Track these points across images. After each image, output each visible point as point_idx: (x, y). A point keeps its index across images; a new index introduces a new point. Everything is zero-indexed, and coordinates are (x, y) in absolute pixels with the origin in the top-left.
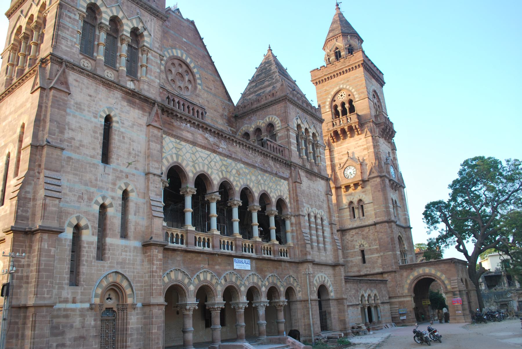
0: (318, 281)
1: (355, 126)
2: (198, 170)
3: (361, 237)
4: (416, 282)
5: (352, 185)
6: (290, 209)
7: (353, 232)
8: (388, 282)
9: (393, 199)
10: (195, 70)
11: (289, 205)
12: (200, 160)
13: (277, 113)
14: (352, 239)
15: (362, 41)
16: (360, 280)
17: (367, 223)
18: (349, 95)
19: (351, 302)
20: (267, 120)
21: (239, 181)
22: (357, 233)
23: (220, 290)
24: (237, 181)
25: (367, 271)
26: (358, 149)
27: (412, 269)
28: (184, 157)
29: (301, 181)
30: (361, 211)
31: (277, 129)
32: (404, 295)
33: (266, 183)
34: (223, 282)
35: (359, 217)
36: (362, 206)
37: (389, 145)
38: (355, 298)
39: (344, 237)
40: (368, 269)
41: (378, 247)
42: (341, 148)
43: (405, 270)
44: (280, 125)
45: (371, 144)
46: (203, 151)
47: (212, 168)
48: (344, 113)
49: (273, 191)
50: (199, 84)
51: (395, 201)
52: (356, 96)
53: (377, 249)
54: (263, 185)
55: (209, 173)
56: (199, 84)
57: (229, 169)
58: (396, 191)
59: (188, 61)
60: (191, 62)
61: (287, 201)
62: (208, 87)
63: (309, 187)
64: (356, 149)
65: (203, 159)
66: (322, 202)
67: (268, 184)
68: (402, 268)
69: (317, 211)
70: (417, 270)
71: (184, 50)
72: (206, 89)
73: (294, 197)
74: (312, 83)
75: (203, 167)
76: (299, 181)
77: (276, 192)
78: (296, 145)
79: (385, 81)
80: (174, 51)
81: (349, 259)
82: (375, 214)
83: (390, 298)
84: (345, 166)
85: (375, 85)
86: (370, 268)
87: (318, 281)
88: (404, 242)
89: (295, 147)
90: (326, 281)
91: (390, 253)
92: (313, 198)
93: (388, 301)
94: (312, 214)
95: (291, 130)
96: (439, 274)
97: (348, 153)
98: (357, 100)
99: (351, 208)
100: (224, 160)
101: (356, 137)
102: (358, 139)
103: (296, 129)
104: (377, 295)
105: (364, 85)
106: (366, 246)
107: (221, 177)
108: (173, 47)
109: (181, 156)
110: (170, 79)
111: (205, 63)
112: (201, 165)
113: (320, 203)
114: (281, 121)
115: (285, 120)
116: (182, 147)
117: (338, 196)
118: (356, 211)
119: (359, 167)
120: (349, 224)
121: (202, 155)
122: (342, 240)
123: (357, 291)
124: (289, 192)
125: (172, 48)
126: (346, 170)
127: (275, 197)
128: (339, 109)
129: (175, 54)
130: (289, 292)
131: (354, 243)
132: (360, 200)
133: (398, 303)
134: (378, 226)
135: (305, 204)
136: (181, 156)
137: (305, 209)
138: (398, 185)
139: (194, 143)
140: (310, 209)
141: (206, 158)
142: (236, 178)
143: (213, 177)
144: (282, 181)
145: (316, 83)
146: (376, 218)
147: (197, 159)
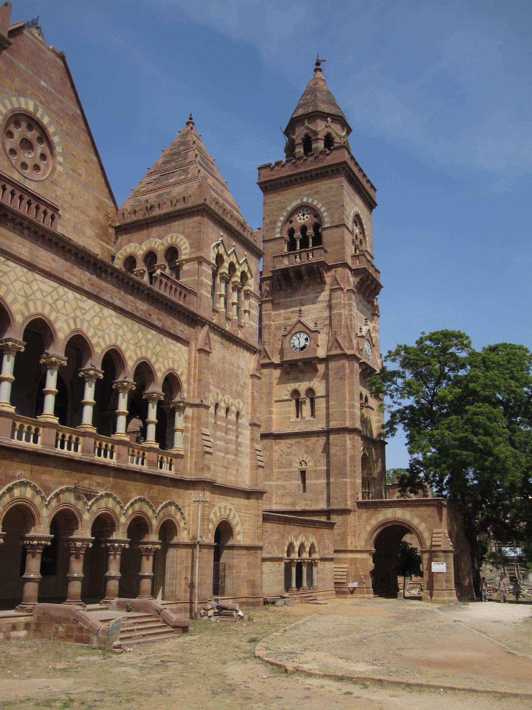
0: (218, 515)
2: (33, 311)
3: (304, 449)
4: (379, 530)
6: (187, 392)
8: (335, 527)
10: (56, 139)
11: (185, 386)
12: (39, 294)
13: (186, 231)
14: (289, 450)
15: (349, 131)
16: (290, 519)
17: (315, 429)
19: (270, 553)
20: (168, 240)
21: (103, 337)
22: (299, 443)
23: (45, 515)
24: (99, 338)
25: (306, 504)
28: (11, 287)
29: (211, 349)
31: (183, 257)
33: (150, 345)
34: (54, 503)
37: (369, 307)
38: (278, 547)
42: (291, 301)
43: (364, 510)
44: (188, 251)
46: (46, 280)
47: (58, 311)
48: (304, 243)
49: (161, 359)
50: (60, 164)
52: (326, 220)
54: (143, 349)
55: (52, 318)
56: (60, 164)
57: (88, 317)
59: (46, 121)
60: (50, 123)
61: (183, 378)
62: (74, 171)
63: (224, 359)
65: (45, 294)
66: (241, 386)
67: (154, 347)
68: (361, 505)
69: (231, 400)
71: (41, 102)
72: (71, 173)
73: (195, 374)
74: (258, 186)
75: (43, 307)
76: (207, 348)
77: (166, 362)
78: (210, 289)
79: (377, 201)
80: (22, 100)
84: (293, 332)
86: (311, 501)
87: (218, 515)
89: (208, 292)
90: (231, 516)
92: (227, 379)
94: (222, 404)
95: (204, 263)
98: (327, 225)
100: (81, 301)
103: (214, 262)
104: (316, 545)
106: (310, 466)
107: (73, 327)
108: (21, 93)
109: (5, 285)
110: (8, 148)
111: (75, 129)
112: (39, 304)
113: (239, 388)
114: (191, 245)
115: (197, 244)
116: (9, 269)
121: (43, 286)
123: (283, 536)
124: (189, 364)
125: (19, 95)
127: (163, 370)
128: (298, 234)
129: (24, 106)
130: (168, 529)
131: (292, 457)
135: (211, 387)
136: (5, 285)
137: (211, 395)
139: (31, 267)
140: (220, 396)
141: (50, 293)
142: (98, 331)
143: (57, 326)
144: (179, 345)
147: (33, 293)
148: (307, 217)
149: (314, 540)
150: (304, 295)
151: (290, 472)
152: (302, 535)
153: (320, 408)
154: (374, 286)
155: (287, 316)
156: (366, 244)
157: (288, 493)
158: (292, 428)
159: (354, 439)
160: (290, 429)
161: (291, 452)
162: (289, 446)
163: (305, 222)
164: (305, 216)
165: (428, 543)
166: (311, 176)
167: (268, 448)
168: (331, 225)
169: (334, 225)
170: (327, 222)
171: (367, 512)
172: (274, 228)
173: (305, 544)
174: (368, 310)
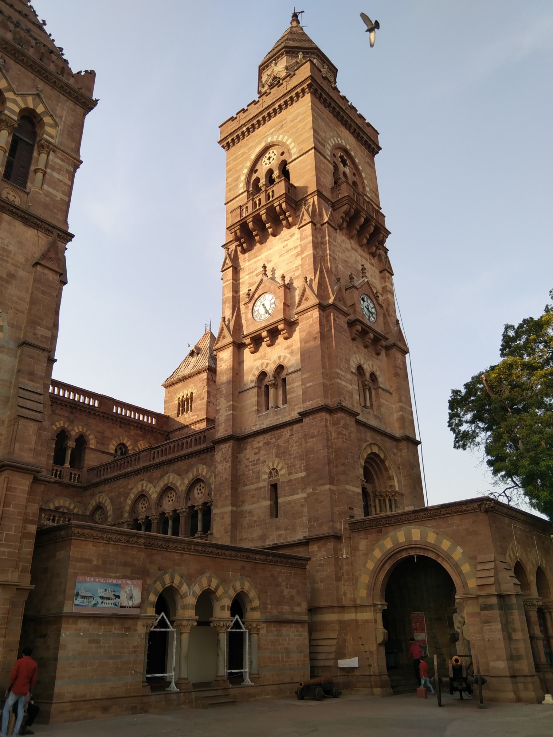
1: (280, 205)
3: (274, 451)
4: (387, 567)
5: (264, 334)
7: (259, 442)
9: (365, 367)
14: (257, 457)
17: (288, 419)
18: (283, 154)
22: (268, 443)
25: (280, 536)
26: (288, 256)
27: (380, 532)
30: (280, 392)
32: (358, 602)
35: (277, 407)
36: (284, 380)
37: (375, 261)
39: (242, 455)
40: (282, 532)
41: (303, 474)
42: (256, 262)
45: (310, 238)
51: (373, 375)
52: (293, 152)
53: (303, 478)
58: (378, 354)
64: (282, 258)
68: (357, 527)
70: (391, 534)
74: (219, 146)
79: (381, 144)
81: (247, 507)
82: (304, 393)
83: (312, 610)
85: (348, 140)
86: (286, 529)
88: (392, 472)
91: (328, 487)
93: (306, 618)
96: (446, 545)
97: (264, 267)
98: (293, 158)
99: (263, 388)
101: (285, 232)
102: (288, 237)
104: (252, 594)
105: (311, 125)
117: (238, 361)
118: (272, 391)
119: (282, 291)
120: (253, 422)
122: (235, 460)
126: (258, 303)
132: (280, 368)
133: (337, 627)
134: (306, 420)
138: (387, 343)
145: (228, 144)
146: (304, 401)
148: (273, 159)
149: (247, 586)
150: (270, 249)
151: (257, 489)
152: (208, 574)
153: (293, 388)
154: (372, 228)
155: (251, 281)
156: (364, 188)
157: (255, 522)
158: (260, 424)
159: (340, 423)
160: (257, 426)
161: (258, 460)
162: (256, 451)
163: (271, 166)
164: (271, 159)
165: (472, 583)
166: (274, 110)
167: (228, 458)
168: (298, 155)
169: (301, 153)
170: (294, 154)
171: (367, 538)
172: (237, 186)
173: (220, 592)
174: (372, 265)
